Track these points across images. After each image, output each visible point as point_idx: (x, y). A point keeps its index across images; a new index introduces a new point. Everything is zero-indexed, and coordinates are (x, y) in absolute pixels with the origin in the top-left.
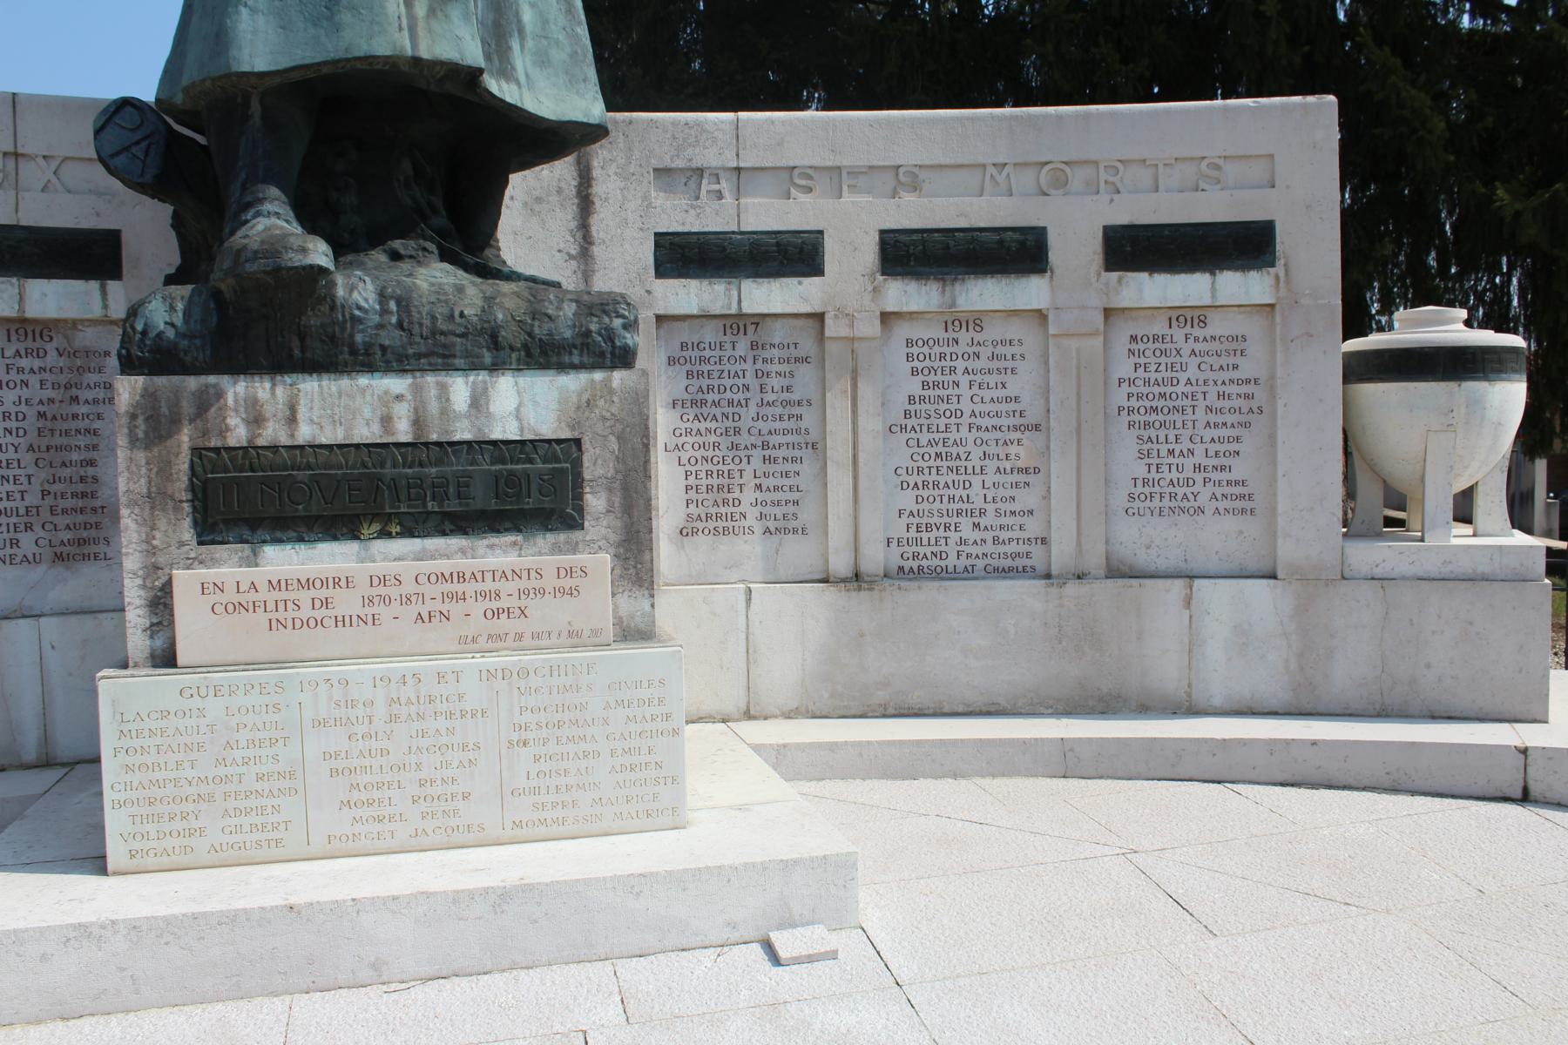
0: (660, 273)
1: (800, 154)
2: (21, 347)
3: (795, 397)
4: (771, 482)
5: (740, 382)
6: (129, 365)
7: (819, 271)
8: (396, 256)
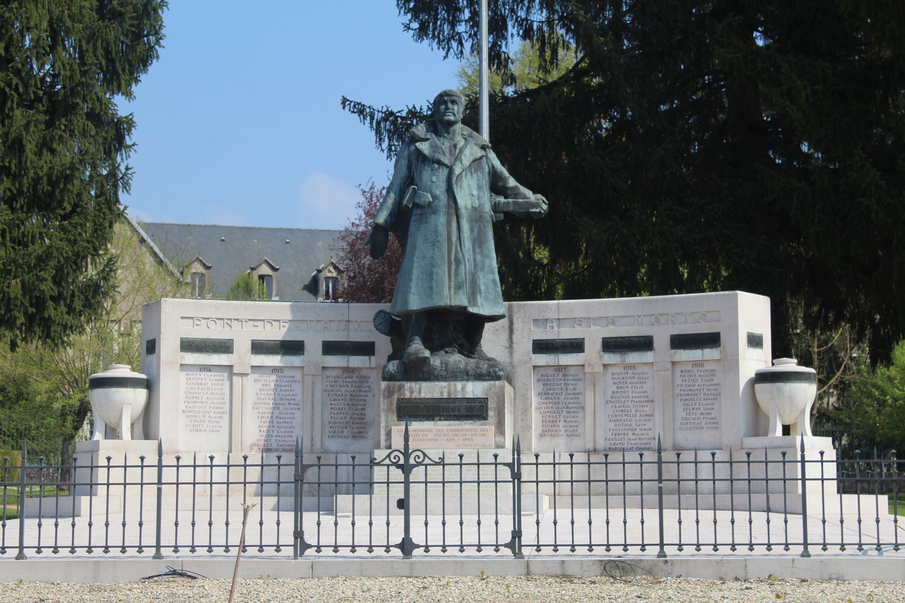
0: (534, 352)
1: (578, 314)
3: (577, 392)
6: (384, 379)
7: (583, 351)
8: (447, 352)
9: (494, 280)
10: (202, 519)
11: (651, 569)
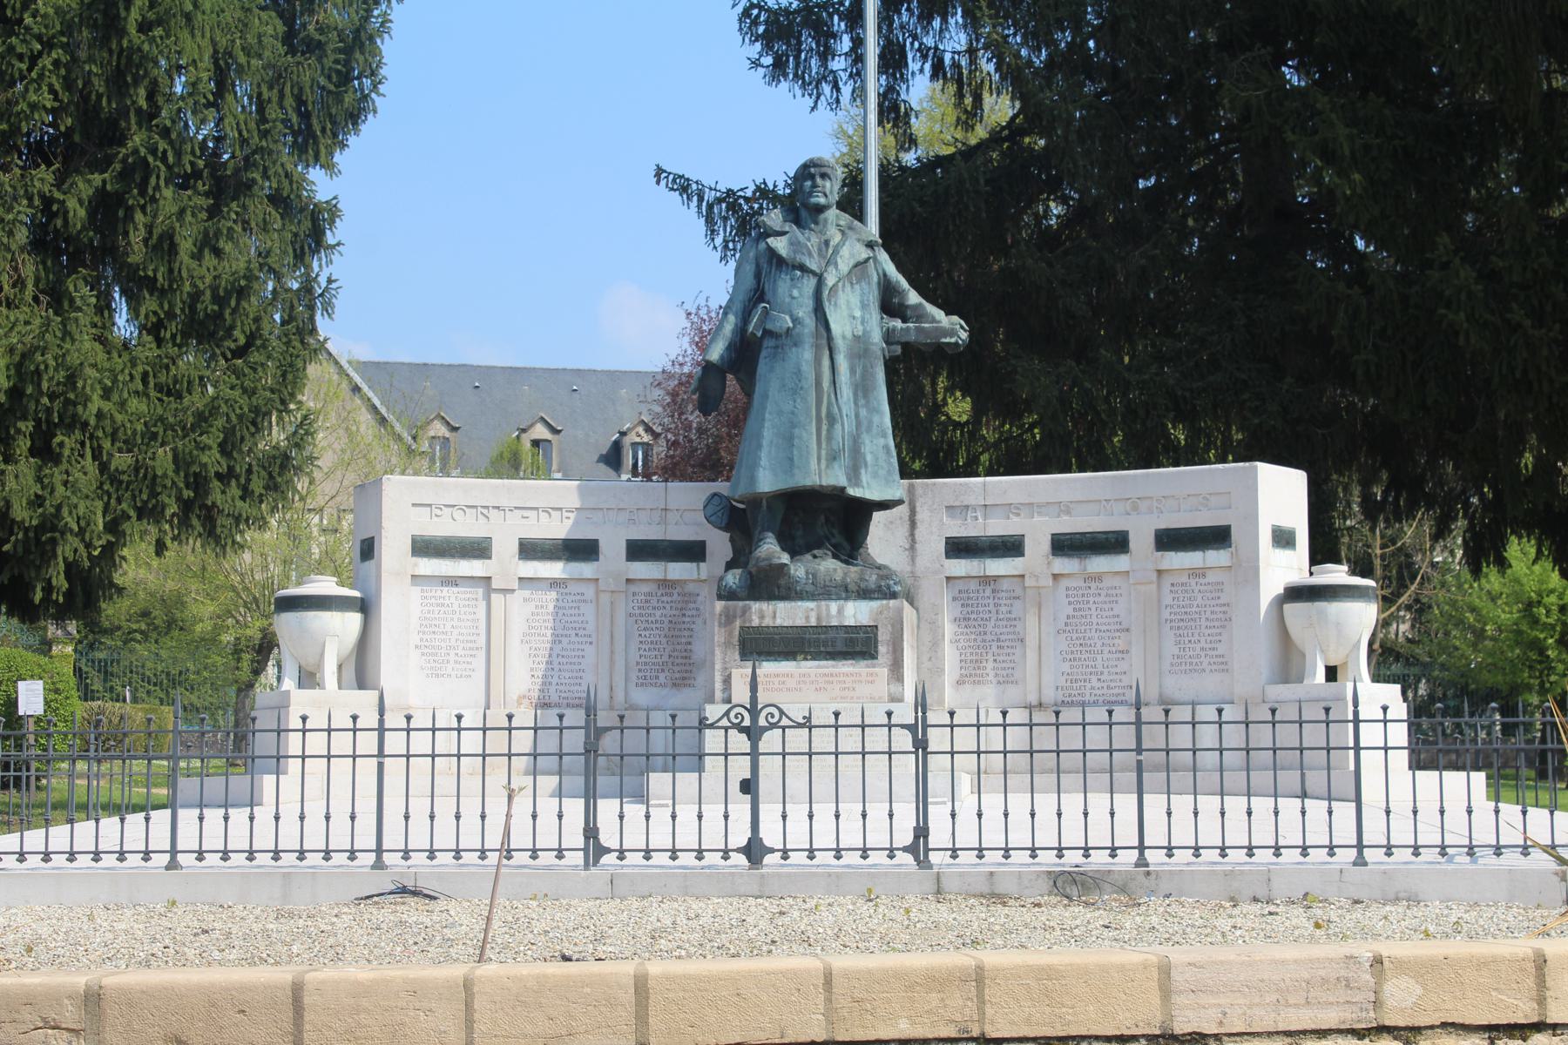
0: (948, 557)
1: (1015, 497)
6: (720, 597)
8: (815, 557)
9: (886, 447)
10: (445, 809)
11: (1125, 885)
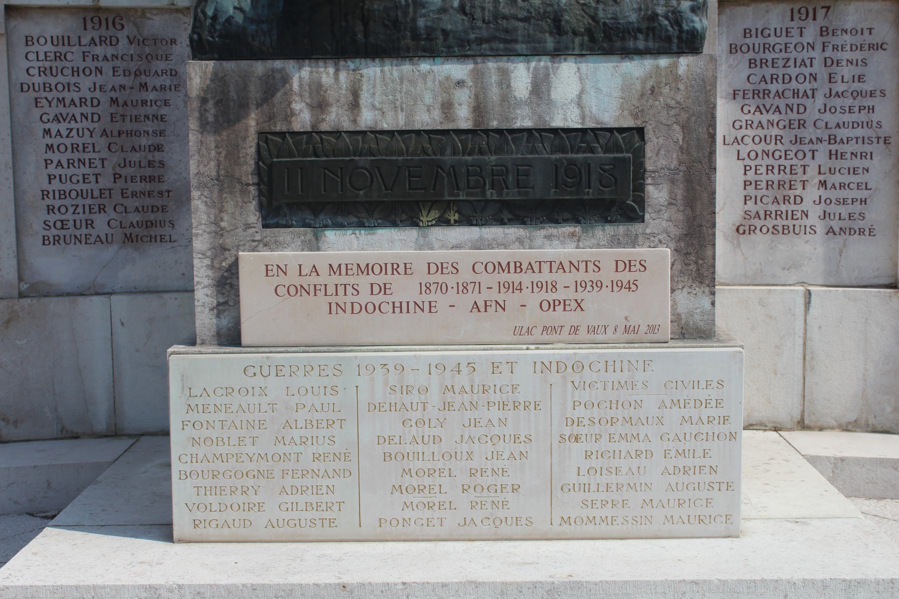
2: (96, 35)
3: (867, 87)
4: (837, 179)
5: (807, 71)
6: (200, 50)
